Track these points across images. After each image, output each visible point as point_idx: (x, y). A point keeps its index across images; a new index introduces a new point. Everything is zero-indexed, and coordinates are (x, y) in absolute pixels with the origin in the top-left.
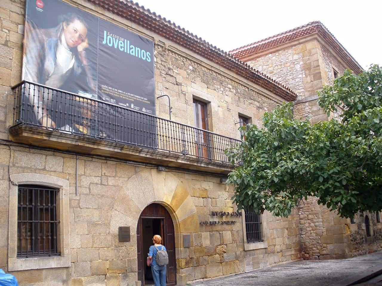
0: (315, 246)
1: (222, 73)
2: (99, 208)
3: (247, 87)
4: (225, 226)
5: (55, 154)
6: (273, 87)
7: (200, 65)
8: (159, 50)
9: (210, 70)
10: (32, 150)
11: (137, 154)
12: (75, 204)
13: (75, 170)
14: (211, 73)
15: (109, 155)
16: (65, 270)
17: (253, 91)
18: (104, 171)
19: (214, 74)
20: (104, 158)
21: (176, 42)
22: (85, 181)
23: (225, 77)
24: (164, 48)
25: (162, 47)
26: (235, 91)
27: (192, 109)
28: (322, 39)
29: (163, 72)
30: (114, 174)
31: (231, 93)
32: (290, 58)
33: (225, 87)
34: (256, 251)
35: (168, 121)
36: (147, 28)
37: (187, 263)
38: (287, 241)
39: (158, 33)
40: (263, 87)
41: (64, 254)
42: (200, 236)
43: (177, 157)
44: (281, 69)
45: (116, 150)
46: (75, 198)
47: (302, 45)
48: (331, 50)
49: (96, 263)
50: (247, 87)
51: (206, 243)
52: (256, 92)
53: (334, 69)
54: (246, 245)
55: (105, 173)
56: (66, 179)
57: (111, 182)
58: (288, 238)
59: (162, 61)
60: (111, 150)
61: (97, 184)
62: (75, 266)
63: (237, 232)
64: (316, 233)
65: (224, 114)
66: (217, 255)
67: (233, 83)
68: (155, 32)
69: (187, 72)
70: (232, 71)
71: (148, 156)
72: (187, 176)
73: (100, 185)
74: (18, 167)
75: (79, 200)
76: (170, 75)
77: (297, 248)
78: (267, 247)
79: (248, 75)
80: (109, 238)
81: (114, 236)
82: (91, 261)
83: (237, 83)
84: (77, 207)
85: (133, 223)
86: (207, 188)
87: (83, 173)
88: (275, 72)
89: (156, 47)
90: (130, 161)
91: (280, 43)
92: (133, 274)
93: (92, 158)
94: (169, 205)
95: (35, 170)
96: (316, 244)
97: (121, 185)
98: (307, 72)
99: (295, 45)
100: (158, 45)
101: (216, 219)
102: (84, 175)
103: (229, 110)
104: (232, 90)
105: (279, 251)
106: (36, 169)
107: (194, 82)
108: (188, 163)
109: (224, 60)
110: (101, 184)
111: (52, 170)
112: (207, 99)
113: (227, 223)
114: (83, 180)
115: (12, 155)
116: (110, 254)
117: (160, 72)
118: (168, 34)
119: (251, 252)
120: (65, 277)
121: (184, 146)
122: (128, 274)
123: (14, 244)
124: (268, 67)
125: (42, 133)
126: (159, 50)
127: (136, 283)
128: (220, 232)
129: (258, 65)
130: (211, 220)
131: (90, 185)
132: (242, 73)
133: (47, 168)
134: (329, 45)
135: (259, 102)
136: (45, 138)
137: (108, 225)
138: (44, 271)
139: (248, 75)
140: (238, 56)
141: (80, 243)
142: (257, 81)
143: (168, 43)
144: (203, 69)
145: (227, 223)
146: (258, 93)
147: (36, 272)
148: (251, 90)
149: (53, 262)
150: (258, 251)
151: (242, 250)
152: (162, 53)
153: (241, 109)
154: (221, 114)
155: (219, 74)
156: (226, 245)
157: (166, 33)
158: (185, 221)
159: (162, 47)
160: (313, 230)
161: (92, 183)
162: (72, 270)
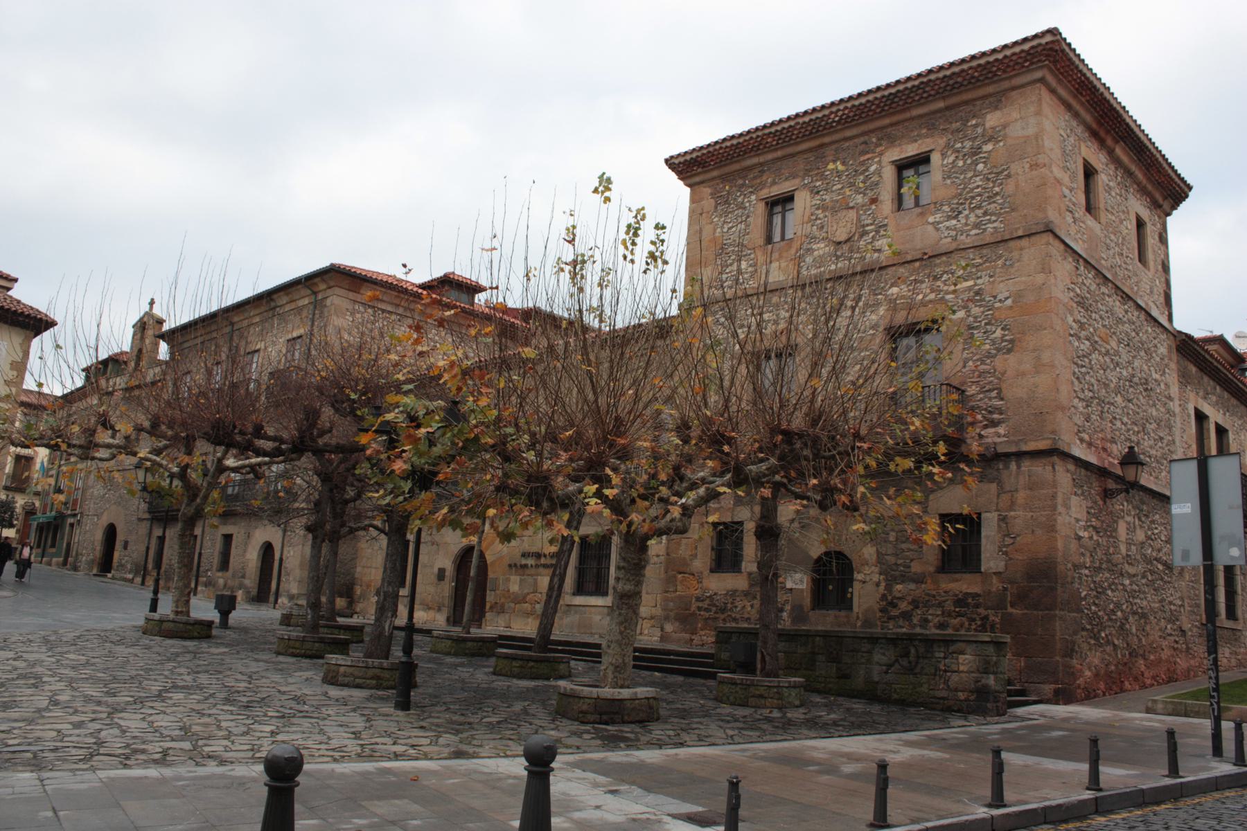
28: (706, 172)
37: (491, 608)
42: (508, 580)
48: (749, 162)
130: (524, 562)
137: (432, 567)
150: (592, 609)
158: (492, 563)
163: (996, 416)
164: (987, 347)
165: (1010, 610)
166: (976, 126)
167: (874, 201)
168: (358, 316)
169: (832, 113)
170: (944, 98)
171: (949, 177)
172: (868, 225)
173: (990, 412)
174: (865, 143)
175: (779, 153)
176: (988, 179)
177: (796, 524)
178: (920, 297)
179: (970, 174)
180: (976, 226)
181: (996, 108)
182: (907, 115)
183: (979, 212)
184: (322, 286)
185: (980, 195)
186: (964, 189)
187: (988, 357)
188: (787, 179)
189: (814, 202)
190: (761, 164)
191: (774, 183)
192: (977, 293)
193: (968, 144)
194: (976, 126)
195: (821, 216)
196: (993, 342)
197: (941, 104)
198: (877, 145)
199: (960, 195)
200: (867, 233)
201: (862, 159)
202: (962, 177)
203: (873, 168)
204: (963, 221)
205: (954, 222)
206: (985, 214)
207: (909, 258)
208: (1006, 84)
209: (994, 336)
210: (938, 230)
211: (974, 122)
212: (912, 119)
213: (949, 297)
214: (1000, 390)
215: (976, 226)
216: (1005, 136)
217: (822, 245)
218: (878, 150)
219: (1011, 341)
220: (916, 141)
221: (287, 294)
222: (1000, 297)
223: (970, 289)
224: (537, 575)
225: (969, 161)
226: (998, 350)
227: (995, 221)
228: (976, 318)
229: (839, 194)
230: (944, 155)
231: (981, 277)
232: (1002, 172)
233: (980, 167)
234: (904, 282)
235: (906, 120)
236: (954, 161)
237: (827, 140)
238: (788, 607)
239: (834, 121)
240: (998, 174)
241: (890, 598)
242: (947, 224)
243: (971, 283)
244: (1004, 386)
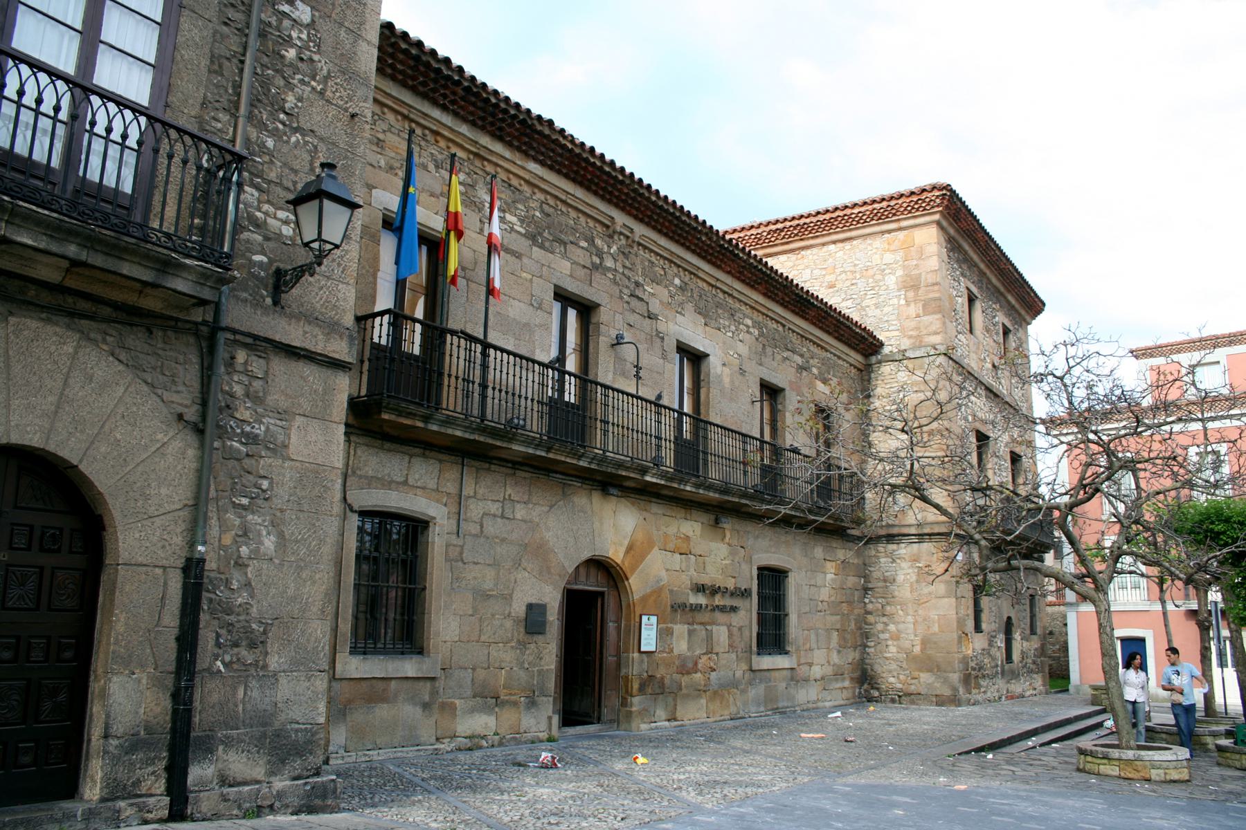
0: (895, 674)
1: (735, 294)
2: (495, 564)
3: (782, 324)
4: (718, 615)
5: (427, 453)
6: (835, 325)
7: (695, 274)
8: (620, 243)
9: (713, 286)
10: (387, 445)
11: (574, 462)
12: (454, 553)
13: (458, 487)
14: (714, 292)
15: (520, 460)
16: (428, 684)
17: (794, 331)
18: (509, 491)
19: (721, 295)
20: (510, 465)
21: (654, 228)
22: (475, 509)
23: (740, 301)
24: (630, 241)
25: (628, 237)
26: (757, 333)
27: (672, 366)
29: (626, 291)
30: (526, 498)
31: (748, 336)
32: (876, 259)
33: (739, 324)
34: (773, 673)
35: (633, 396)
36: (602, 198)
38: (835, 658)
39: (623, 209)
40: (814, 324)
41: (429, 652)
43: (644, 471)
44: (854, 281)
45: (539, 453)
46: (455, 543)
47: (905, 232)
48: (967, 247)
50: (782, 324)
52: (798, 334)
53: (968, 288)
54: (754, 657)
55: (510, 495)
56: (441, 503)
57: (520, 512)
58: (839, 652)
59: (624, 267)
60: (531, 451)
61: (495, 516)
62: (446, 677)
63: (740, 629)
64: (898, 647)
65: (732, 382)
66: (699, 675)
67: (756, 313)
68: (617, 206)
69: (670, 291)
70: (756, 289)
71: (593, 466)
72: (656, 508)
73: (499, 520)
74: (360, 477)
75: (462, 547)
76: (638, 297)
77: (857, 675)
78: (795, 666)
79: (787, 299)
80: (508, 624)
81: (517, 621)
82: (474, 669)
83: (763, 314)
84: (457, 561)
85: (553, 599)
86: (690, 534)
87: (472, 494)
88: (839, 286)
89: (616, 237)
90: (556, 472)
91: (858, 222)
92: (545, 699)
93: (490, 463)
94: (618, 565)
95: (389, 484)
96: (895, 670)
97: (537, 520)
98: (911, 294)
99: (889, 232)
100: (621, 233)
101: (701, 600)
102: (474, 497)
103: (742, 372)
104: (751, 330)
105: (818, 676)
106: (392, 482)
107: (680, 313)
108: (663, 482)
109: (743, 267)
110: (503, 517)
111: (419, 484)
112: (702, 349)
113: (722, 609)
114: (471, 507)
115: (352, 452)
116: (507, 656)
117: (621, 291)
118: (642, 212)
119: (763, 673)
120: (427, 698)
121: (659, 447)
122: (536, 698)
124: (824, 273)
125: (415, 415)
126: (620, 243)
127: (550, 718)
128: (709, 627)
129: (802, 267)
131: (482, 517)
132: (776, 295)
133: (411, 481)
134: (963, 237)
135: (802, 356)
136: (420, 424)
137: (508, 598)
138: (393, 682)
139: (787, 299)
140: (760, 239)
141: (457, 633)
142: (803, 311)
143: (640, 230)
144: (701, 284)
145: (722, 609)
146: (802, 336)
147: (380, 683)
148: (789, 329)
149: (409, 667)
150: (776, 674)
151: (745, 667)
152: (626, 251)
153: (765, 370)
154: (726, 380)
155: (730, 295)
156: (717, 654)
157: (637, 209)
158: (644, 599)
159: (628, 237)
160: (892, 638)
161: (487, 514)
162: (440, 684)
224: (713, 623)
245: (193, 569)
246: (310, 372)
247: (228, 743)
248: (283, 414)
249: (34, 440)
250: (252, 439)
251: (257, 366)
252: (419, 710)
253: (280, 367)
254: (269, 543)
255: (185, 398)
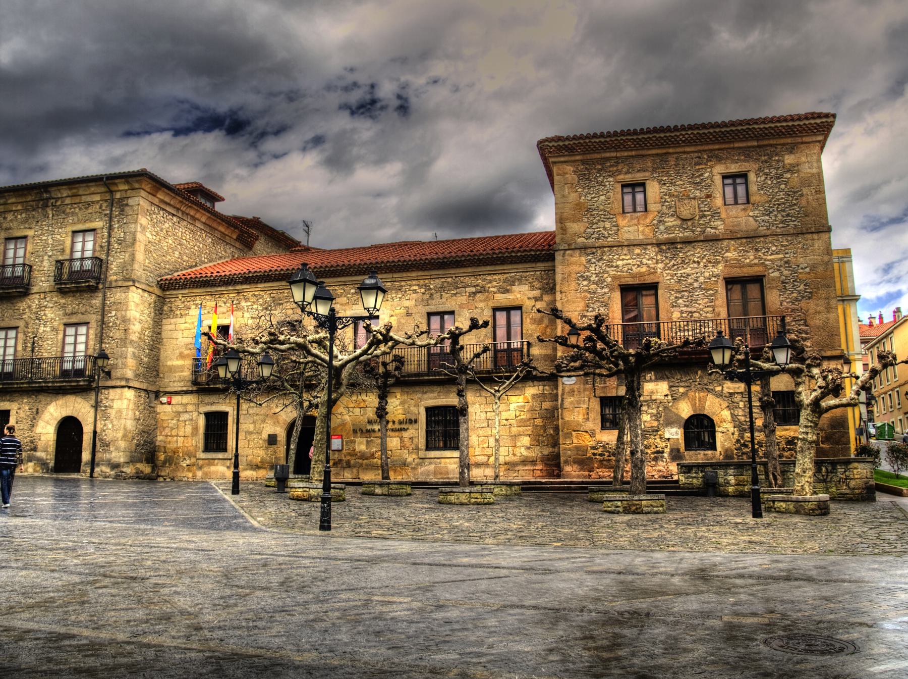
2: (254, 422)
16: (229, 461)
28: (569, 155)
48: (608, 155)
49: (250, 458)
51: (363, 447)
80: (261, 442)
81: (264, 440)
85: (281, 434)
116: (261, 453)
123: (201, 445)
130: (369, 427)
137: (260, 433)
149: (220, 455)
150: (448, 460)
163: (804, 335)
164: (795, 295)
165: (821, 445)
166: (778, 161)
167: (708, 196)
168: (154, 216)
169: (681, 135)
170: (758, 140)
171: (762, 190)
172: (705, 211)
173: (800, 333)
174: (699, 157)
175: (633, 153)
176: (789, 195)
177: (670, 398)
178: (748, 261)
179: (776, 190)
180: (782, 222)
181: (791, 152)
182: (732, 145)
183: (784, 214)
184: (123, 187)
185: (783, 204)
186: (772, 198)
187: (796, 301)
188: (638, 171)
189: (662, 190)
190: (617, 158)
191: (627, 172)
192: (786, 263)
193: (774, 172)
194: (778, 161)
195: (669, 200)
196: (799, 292)
197: (755, 143)
198: (708, 161)
199: (770, 201)
200: (705, 216)
201: (697, 167)
202: (771, 191)
203: (706, 175)
204: (773, 218)
205: (767, 218)
206: (788, 215)
207: (739, 236)
208: (799, 140)
209: (799, 289)
210: (756, 221)
211: (777, 158)
212: (734, 148)
213: (767, 263)
214: (805, 321)
215: (782, 222)
216: (798, 171)
217: (672, 220)
218: (709, 164)
219: (811, 293)
220: (737, 163)
221: (70, 189)
222: (801, 266)
223: (781, 259)
225: (775, 182)
226: (801, 296)
227: (794, 221)
228: (786, 277)
229: (682, 188)
230: (757, 175)
231: (787, 253)
232: (797, 192)
233: (783, 186)
234: (735, 250)
235: (730, 148)
236: (764, 180)
237: (671, 150)
238: (667, 450)
239: (681, 140)
240: (795, 192)
241: (742, 442)
242: (763, 218)
243: (781, 256)
244: (808, 318)
245: (95, 432)
246: (118, 390)
247: (102, 464)
248: (112, 400)
249: (70, 415)
250: (106, 407)
251: (106, 392)
252: (225, 468)
253: (111, 391)
254: (110, 426)
255: (93, 402)
